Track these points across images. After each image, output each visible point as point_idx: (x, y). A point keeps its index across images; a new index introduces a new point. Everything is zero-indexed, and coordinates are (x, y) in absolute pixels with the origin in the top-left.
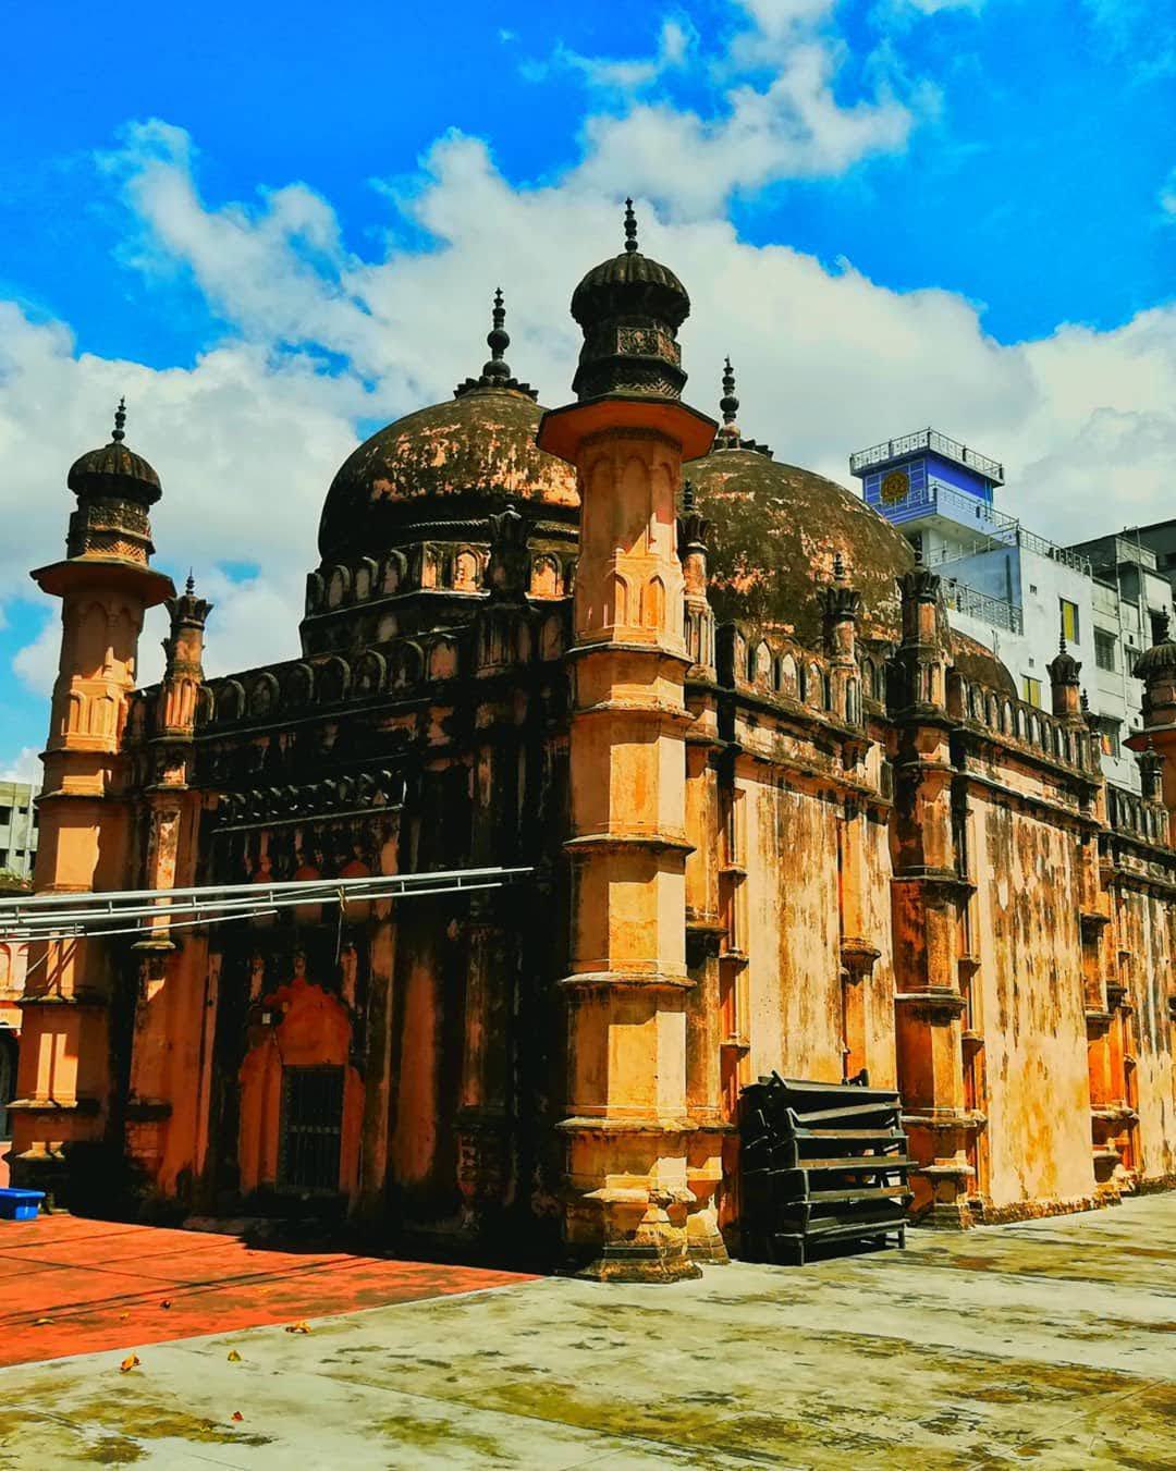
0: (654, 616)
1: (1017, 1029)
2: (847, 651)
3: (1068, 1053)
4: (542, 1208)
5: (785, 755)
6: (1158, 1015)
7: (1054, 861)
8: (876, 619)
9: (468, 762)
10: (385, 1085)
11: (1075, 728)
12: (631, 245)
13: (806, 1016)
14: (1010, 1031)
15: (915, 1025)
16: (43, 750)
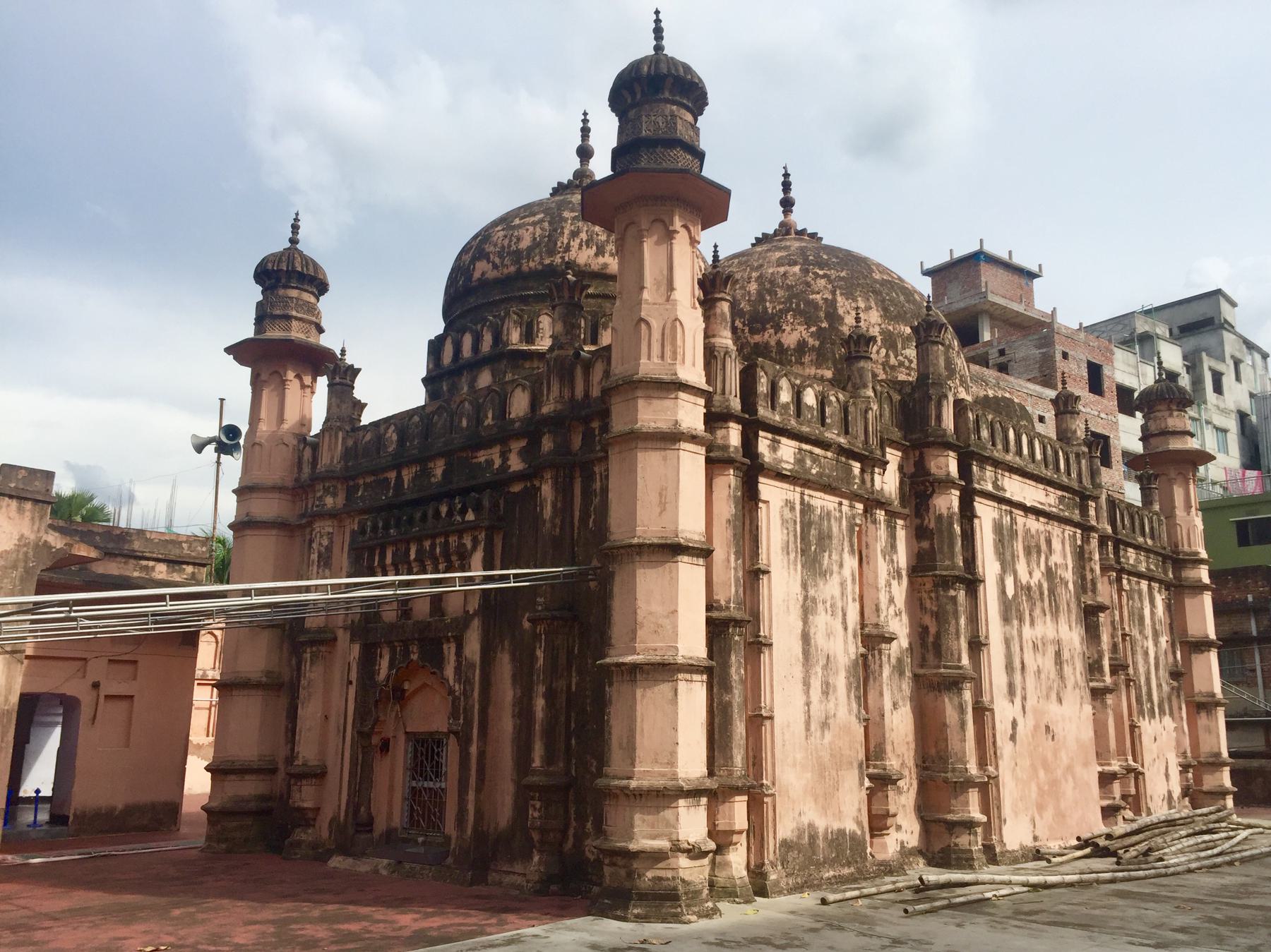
0: (675, 353)
1: (1024, 698)
2: (865, 386)
3: (1074, 717)
5: (808, 471)
6: (1159, 686)
7: (1056, 558)
8: (901, 364)
9: (537, 483)
10: (474, 749)
11: (1075, 449)
12: (658, 48)
13: (827, 690)
14: (1018, 700)
15: (931, 695)
16: (236, 486)
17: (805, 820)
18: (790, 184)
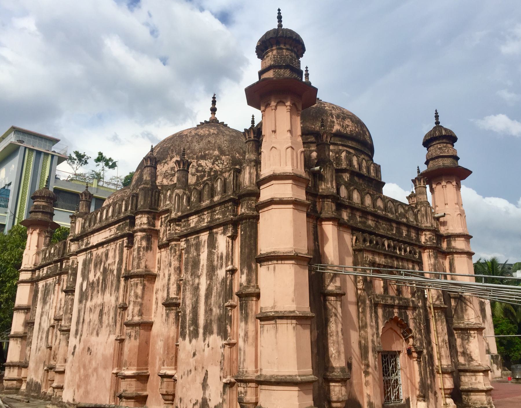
1: (81, 335)
17: (32, 377)
18: (215, 101)
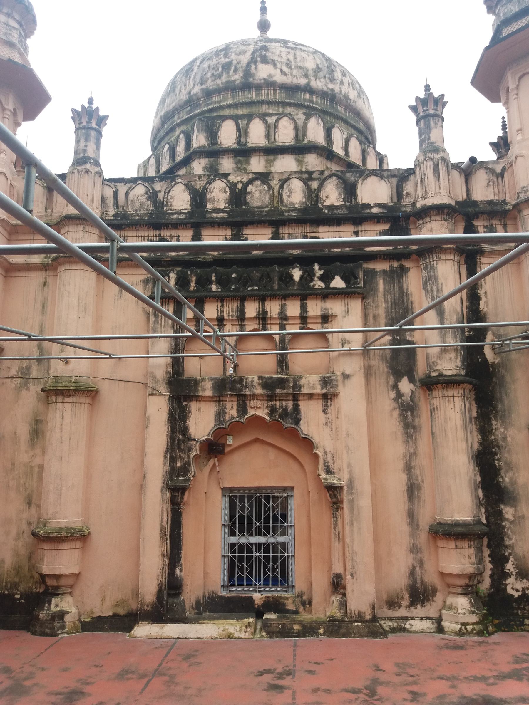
4: (517, 590)
